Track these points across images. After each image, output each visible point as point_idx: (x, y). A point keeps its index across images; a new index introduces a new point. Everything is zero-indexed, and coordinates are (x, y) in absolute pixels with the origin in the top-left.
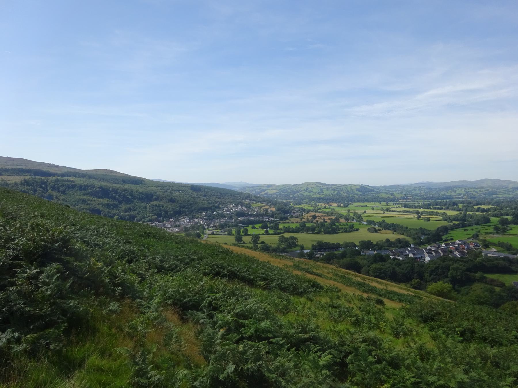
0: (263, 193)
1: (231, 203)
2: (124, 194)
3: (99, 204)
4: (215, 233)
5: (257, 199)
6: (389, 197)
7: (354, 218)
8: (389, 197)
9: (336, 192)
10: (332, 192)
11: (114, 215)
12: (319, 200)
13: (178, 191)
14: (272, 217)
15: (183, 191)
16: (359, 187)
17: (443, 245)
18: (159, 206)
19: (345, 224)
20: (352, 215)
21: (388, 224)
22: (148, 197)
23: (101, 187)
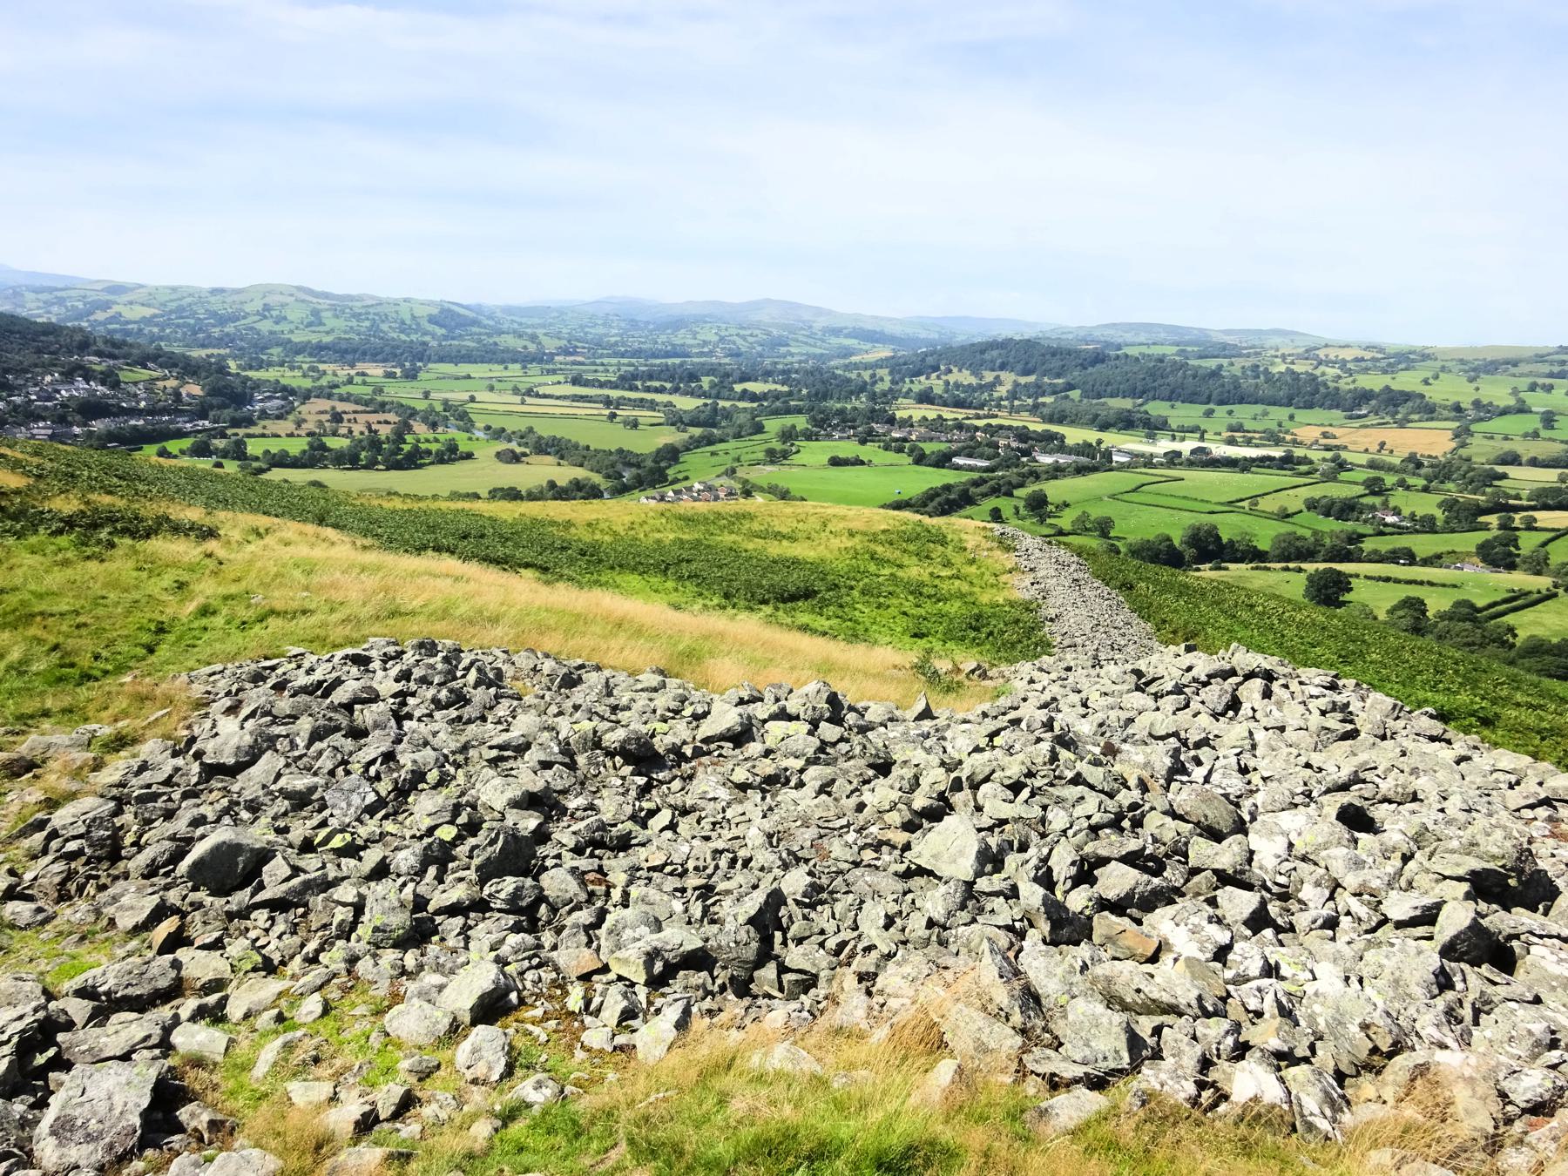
0: (100, 316)
1: (47, 368)
5: (118, 348)
6: (525, 347)
7: (446, 418)
8: (525, 347)
9: (367, 324)
10: (354, 323)
12: (319, 350)
16: (435, 311)
17: (671, 494)
19: (431, 436)
20: (439, 408)
21: (540, 438)
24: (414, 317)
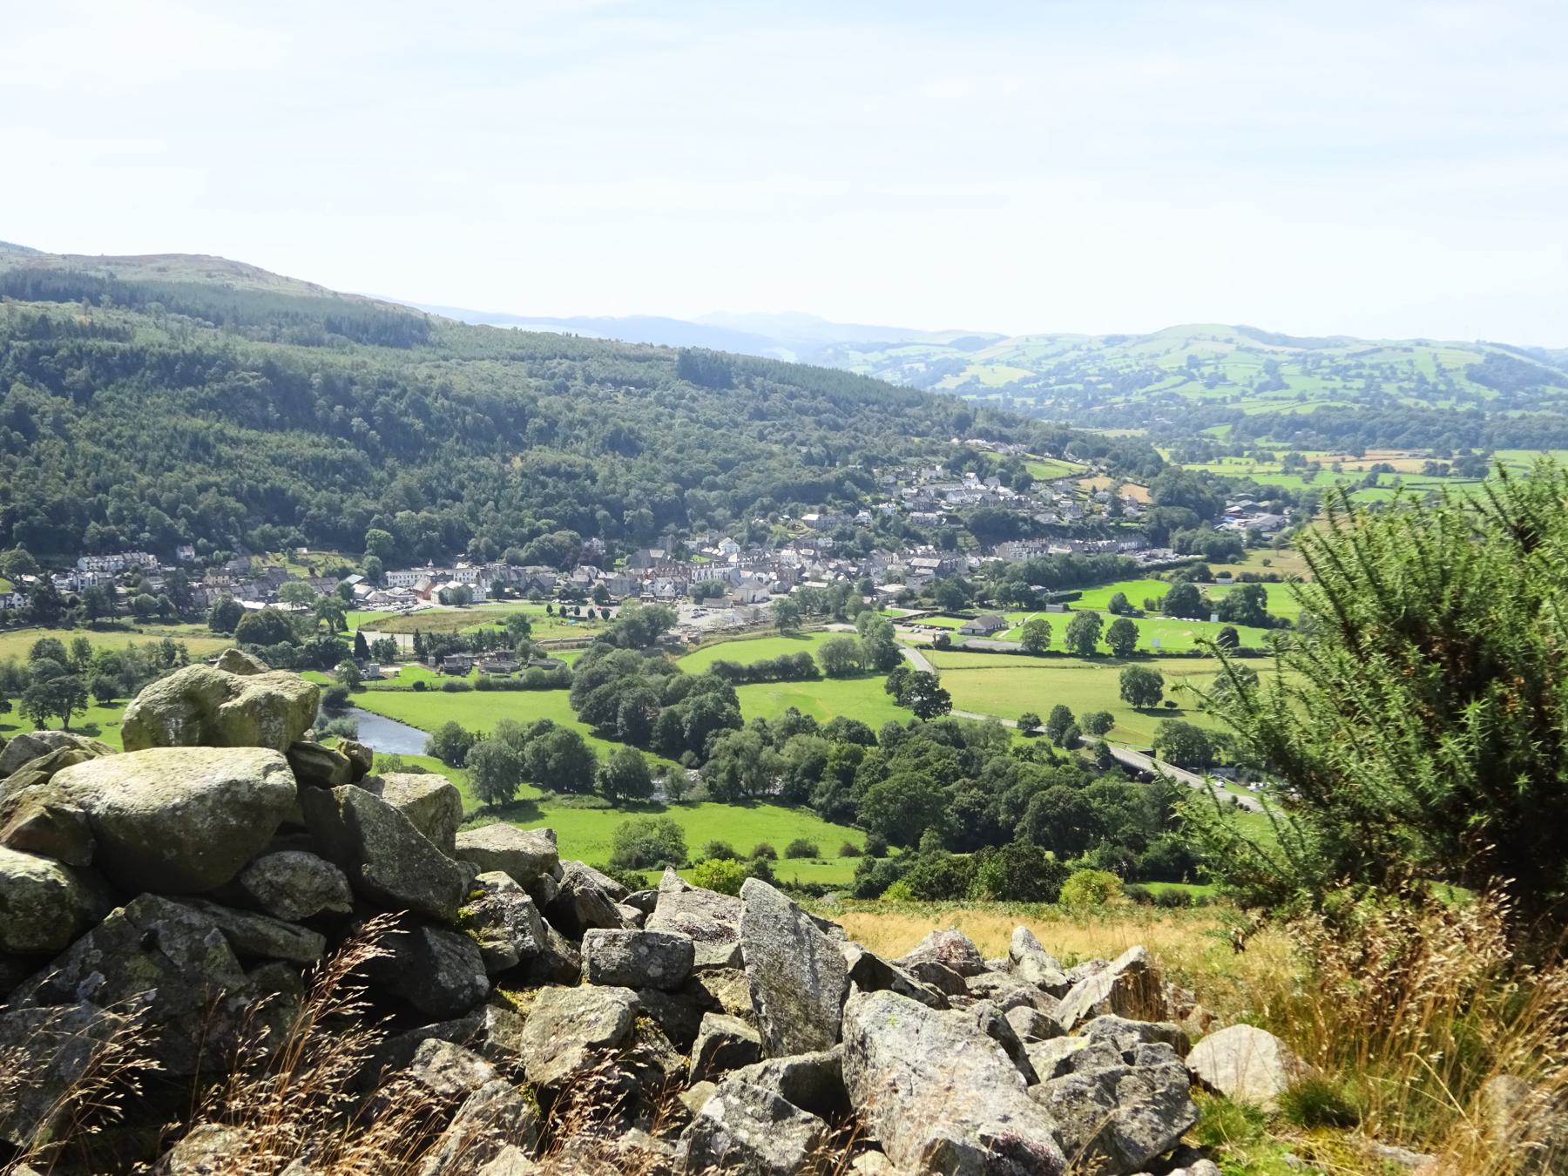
0: (949, 384)
2: (386, 407)
3: (275, 461)
4: (956, 639)
9: (1360, 383)
10: (1338, 383)
11: (364, 519)
12: (1291, 428)
13: (617, 384)
14: (1158, 537)
15: (639, 384)
16: (1479, 360)
18: (571, 476)
22: (505, 424)
23: (269, 369)
24: (1441, 371)
